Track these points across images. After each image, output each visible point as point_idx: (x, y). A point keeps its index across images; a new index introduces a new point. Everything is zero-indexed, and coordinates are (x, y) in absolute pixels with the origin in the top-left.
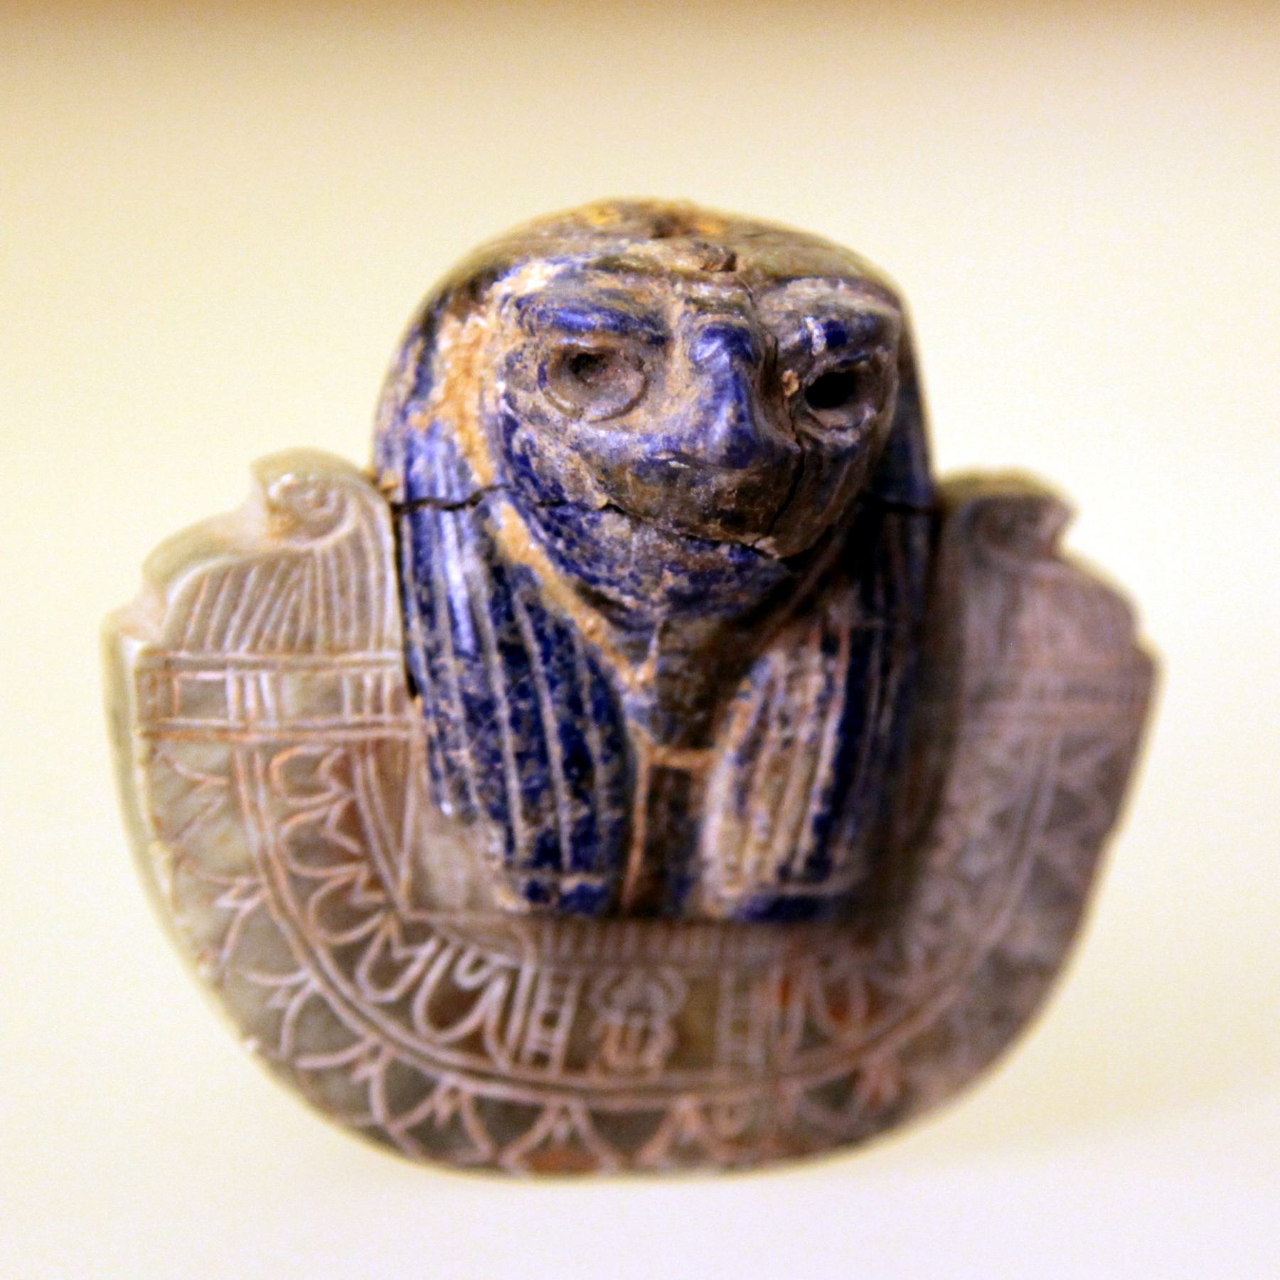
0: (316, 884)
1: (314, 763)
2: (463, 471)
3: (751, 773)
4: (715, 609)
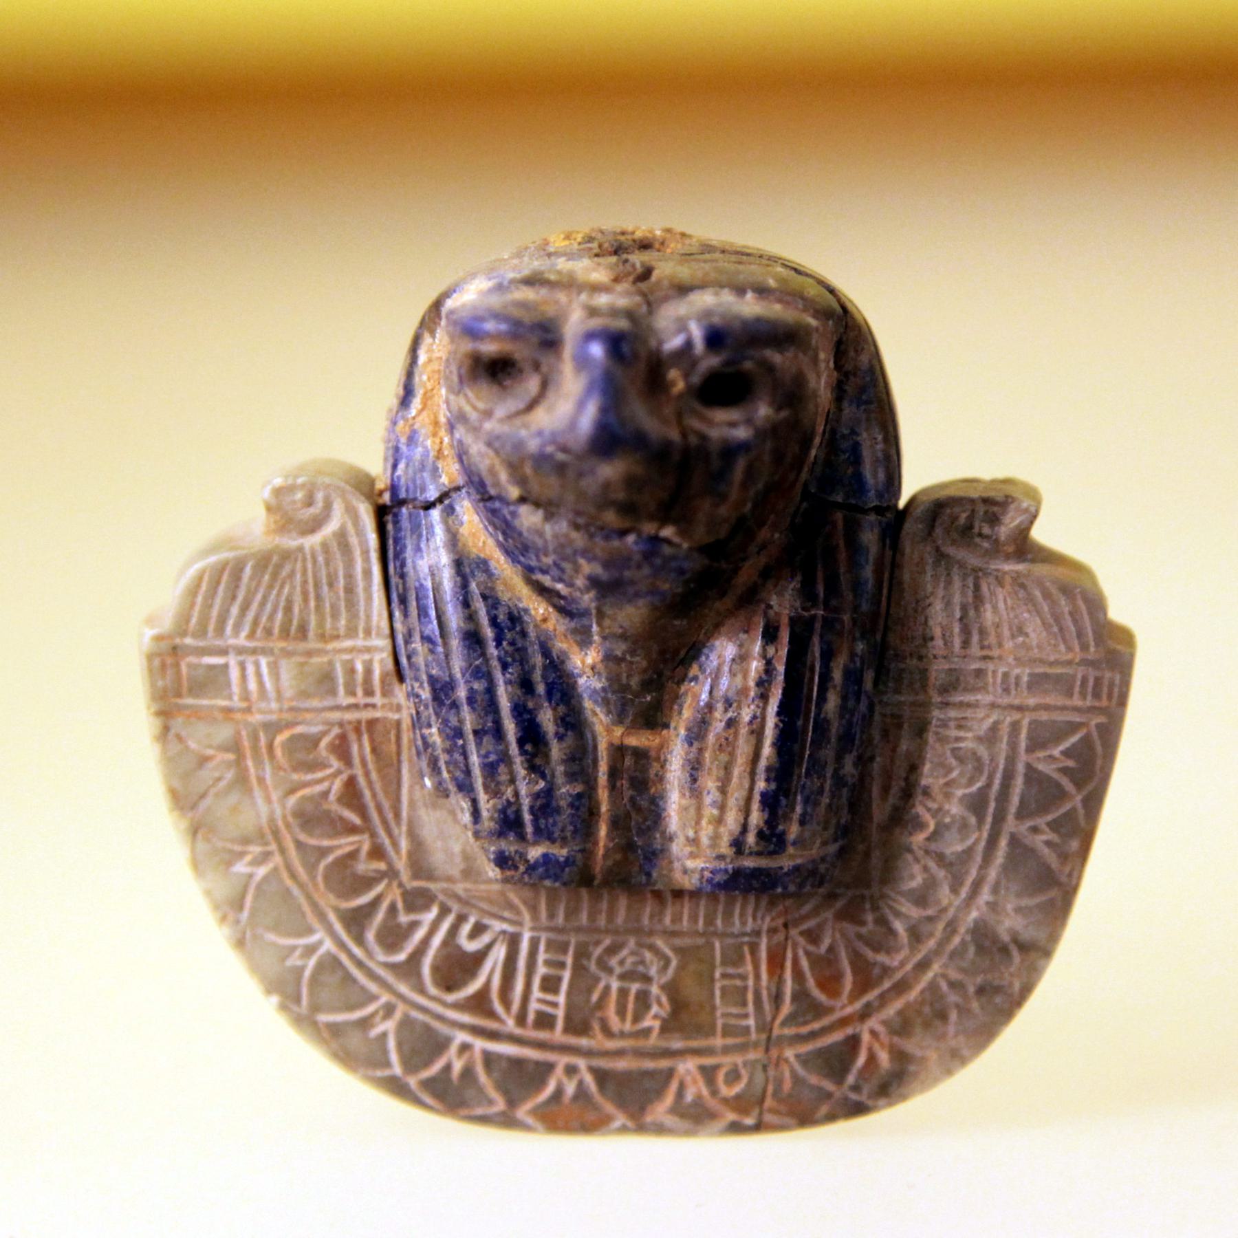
0: (323, 852)
1: (315, 741)
2: (435, 472)
3: (701, 750)
4: (637, 595)
